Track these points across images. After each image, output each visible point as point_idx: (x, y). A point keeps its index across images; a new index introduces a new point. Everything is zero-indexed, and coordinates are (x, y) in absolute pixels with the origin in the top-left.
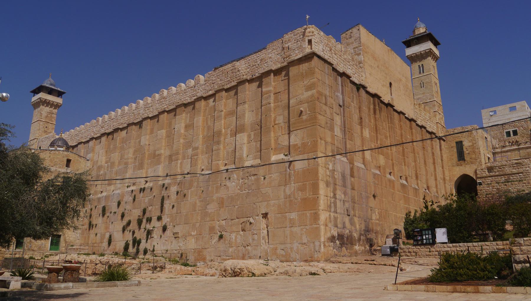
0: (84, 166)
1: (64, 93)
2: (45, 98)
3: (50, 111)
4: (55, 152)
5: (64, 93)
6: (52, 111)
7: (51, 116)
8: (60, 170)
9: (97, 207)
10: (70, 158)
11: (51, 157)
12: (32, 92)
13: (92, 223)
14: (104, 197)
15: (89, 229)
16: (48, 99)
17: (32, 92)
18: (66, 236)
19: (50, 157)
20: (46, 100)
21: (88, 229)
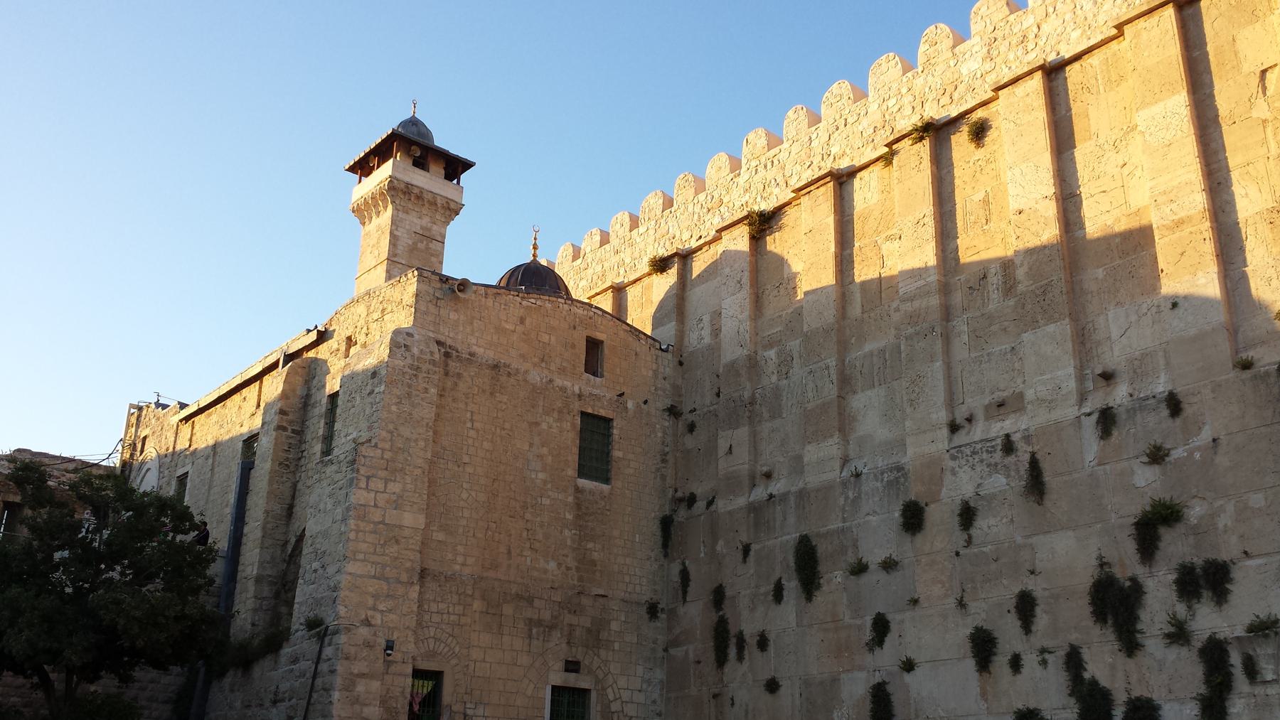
0: (650, 373)
1: (467, 165)
2: (407, 179)
3: (422, 228)
4: (539, 303)
5: (467, 165)
6: (429, 230)
7: (428, 248)
8: (568, 384)
9: (754, 547)
10: (600, 336)
11: (528, 321)
12: (352, 169)
13: (733, 630)
14: (792, 498)
15: (721, 660)
16: (414, 182)
17: (352, 169)
18: (611, 697)
19: (522, 321)
20: (408, 184)
21: (711, 656)
